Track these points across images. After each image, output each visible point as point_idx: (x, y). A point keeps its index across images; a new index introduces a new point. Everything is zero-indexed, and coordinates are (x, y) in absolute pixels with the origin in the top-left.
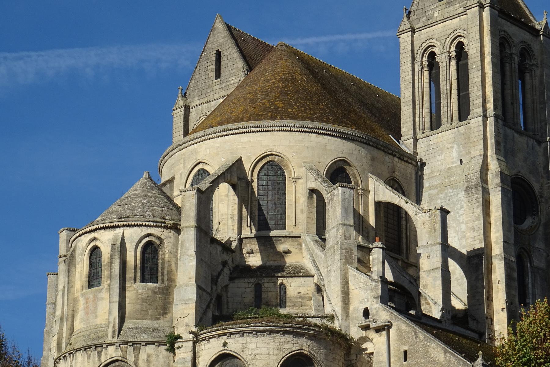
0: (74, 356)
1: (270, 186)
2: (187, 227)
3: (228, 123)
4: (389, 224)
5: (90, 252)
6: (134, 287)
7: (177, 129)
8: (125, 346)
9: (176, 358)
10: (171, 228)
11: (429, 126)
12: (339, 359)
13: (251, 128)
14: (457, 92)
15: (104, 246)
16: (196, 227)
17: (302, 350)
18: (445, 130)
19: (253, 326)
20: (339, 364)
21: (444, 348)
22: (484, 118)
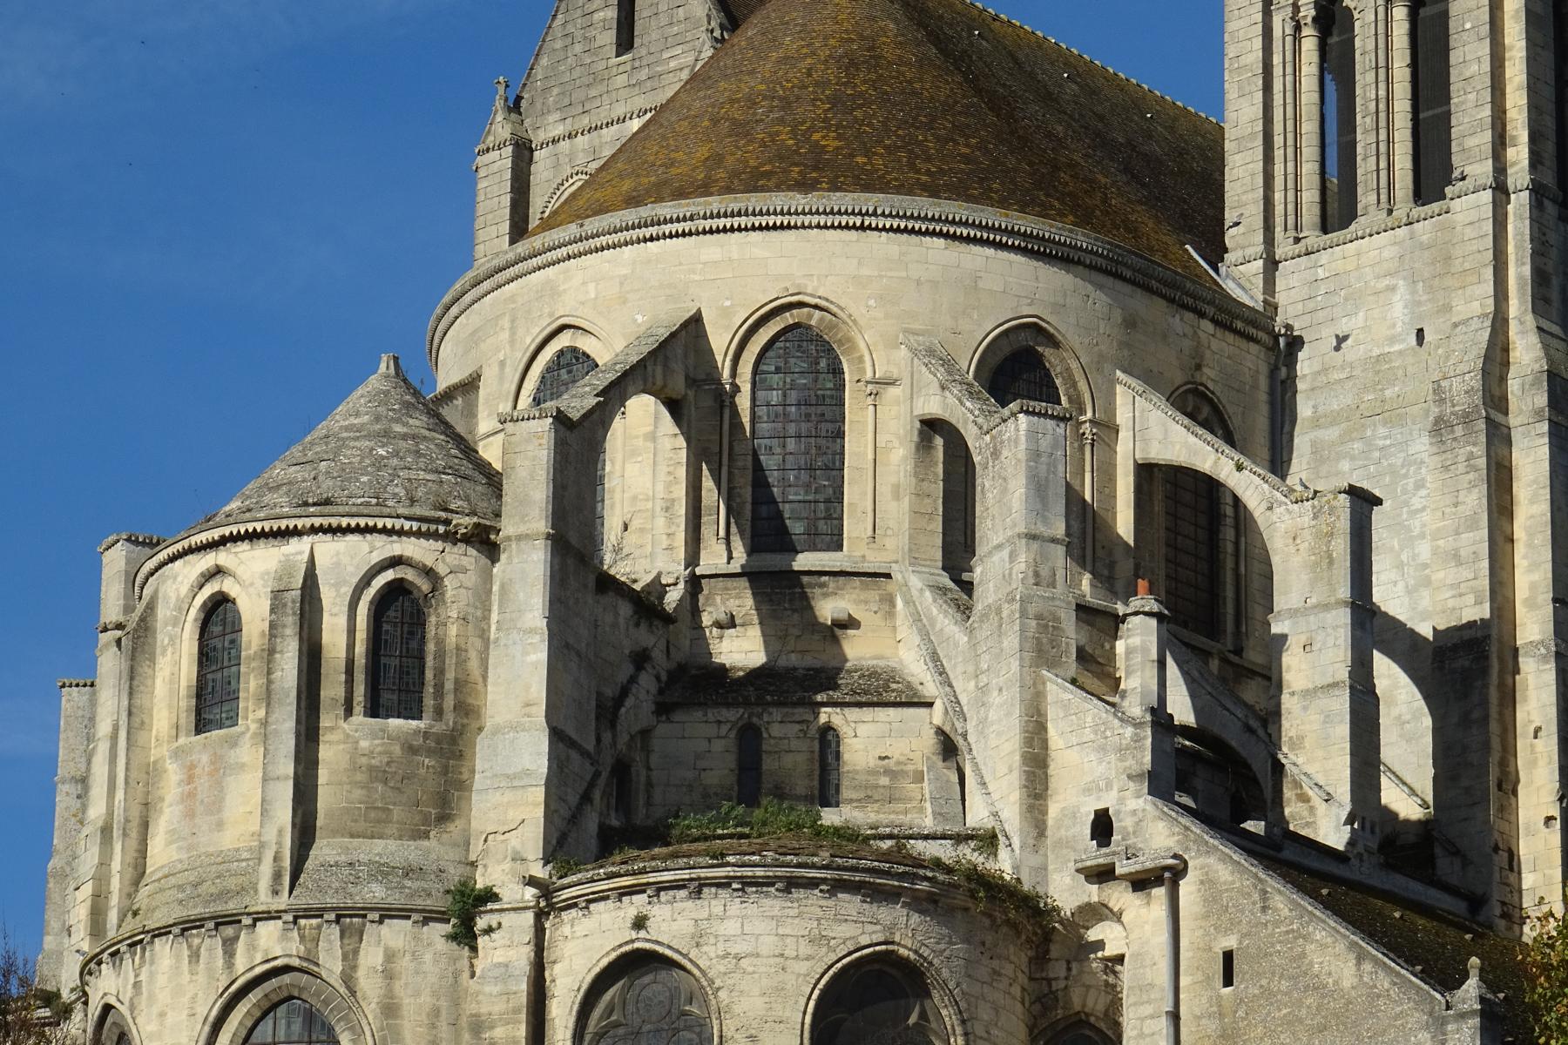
0: (147, 954)
1: (793, 409)
2: (519, 538)
3: (660, 199)
4: (1180, 538)
5: (202, 616)
6: (344, 731)
7: (490, 216)
8: (314, 922)
9: (480, 965)
10: (467, 540)
11: (1317, 220)
12: (1012, 976)
13: (732, 215)
14: (1409, 109)
15: (249, 596)
16: (548, 537)
17: (892, 943)
18: (1368, 231)
19: (734, 865)
20: (1013, 990)
21: (1357, 943)
22: (1498, 193)
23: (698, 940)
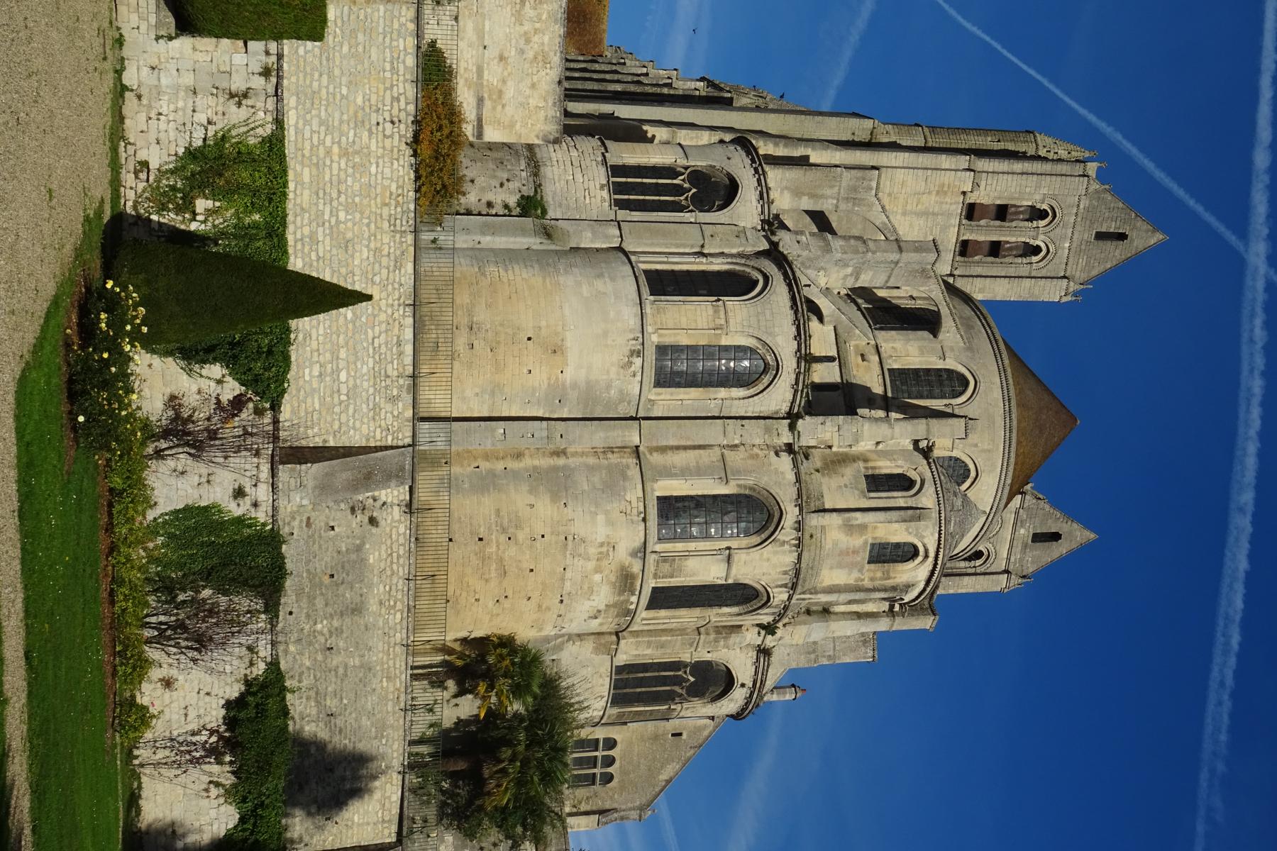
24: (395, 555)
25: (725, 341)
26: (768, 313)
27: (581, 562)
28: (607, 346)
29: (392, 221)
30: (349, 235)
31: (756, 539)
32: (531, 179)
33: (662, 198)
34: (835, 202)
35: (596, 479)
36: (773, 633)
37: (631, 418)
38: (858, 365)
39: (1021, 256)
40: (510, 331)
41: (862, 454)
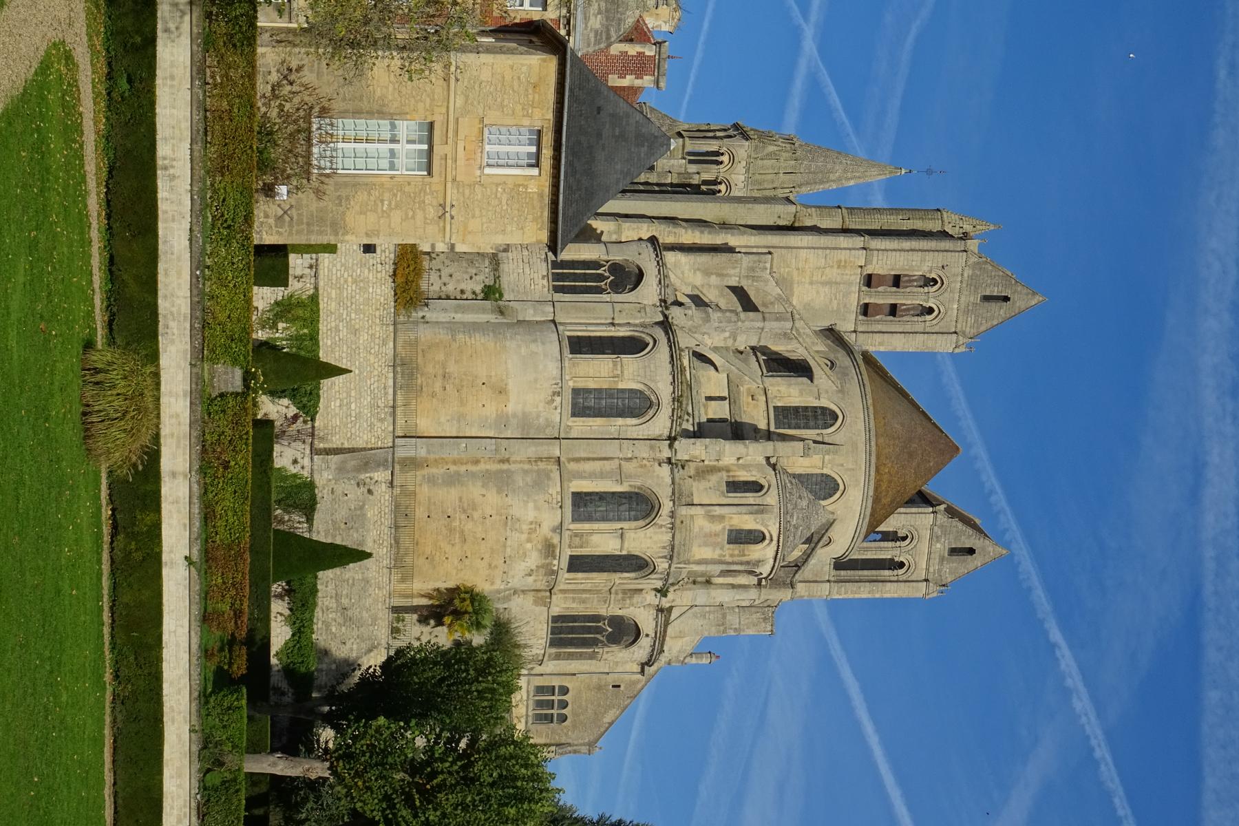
23: (640, 647)
24: (383, 513)
25: (621, 386)
26: (652, 366)
27: (517, 534)
28: (536, 389)
29: (381, 318)
30: (357, 327)
31: (641, 523)
32: (492, 274)
33: (588, 284)
34: (737, 279)
35: (529, 479)
36: (665, 596)
37: (555, 438)
38: (748, 404)
39: (918, 315)
40: (470, 378)
41: (726, 467)
